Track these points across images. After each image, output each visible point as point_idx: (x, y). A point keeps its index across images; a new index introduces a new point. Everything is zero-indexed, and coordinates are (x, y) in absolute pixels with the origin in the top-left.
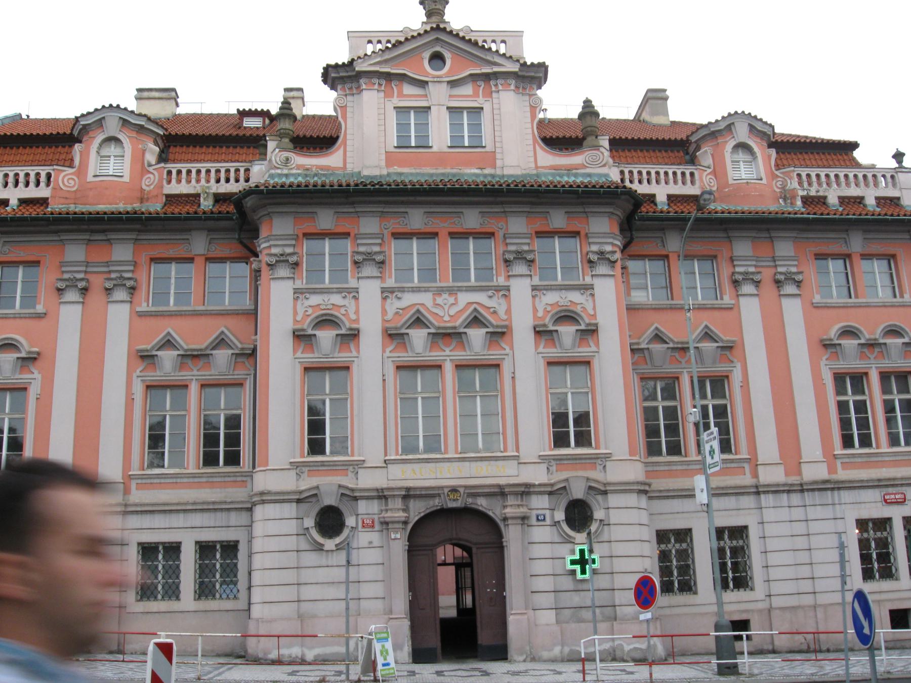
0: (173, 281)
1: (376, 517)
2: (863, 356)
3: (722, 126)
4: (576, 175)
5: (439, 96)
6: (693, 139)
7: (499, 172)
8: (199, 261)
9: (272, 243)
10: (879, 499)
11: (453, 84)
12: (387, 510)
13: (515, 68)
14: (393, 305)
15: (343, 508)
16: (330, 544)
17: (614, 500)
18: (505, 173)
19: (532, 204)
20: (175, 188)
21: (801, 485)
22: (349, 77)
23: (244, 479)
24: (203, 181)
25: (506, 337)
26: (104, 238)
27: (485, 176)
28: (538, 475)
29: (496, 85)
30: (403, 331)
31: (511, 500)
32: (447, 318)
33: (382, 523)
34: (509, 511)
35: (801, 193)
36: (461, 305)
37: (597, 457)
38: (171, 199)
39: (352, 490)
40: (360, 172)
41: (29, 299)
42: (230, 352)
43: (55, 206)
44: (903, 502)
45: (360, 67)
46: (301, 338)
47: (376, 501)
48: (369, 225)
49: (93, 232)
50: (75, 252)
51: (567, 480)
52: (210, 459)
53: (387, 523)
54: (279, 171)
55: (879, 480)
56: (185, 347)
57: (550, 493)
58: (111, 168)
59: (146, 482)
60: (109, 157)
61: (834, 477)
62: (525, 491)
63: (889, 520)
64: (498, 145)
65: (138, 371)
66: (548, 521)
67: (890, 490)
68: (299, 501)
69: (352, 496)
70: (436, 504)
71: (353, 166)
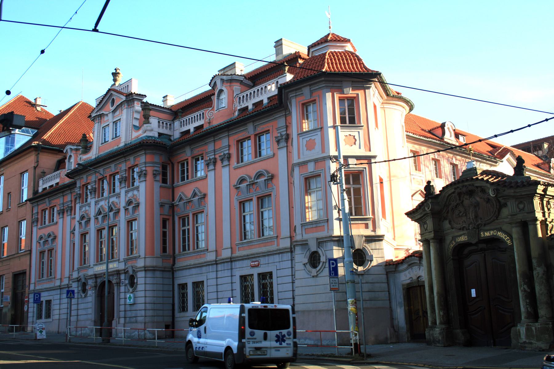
11: (114, 111)
35: (239, 108)
49: (63, 192)
55: (248, 255)
61: (234, 255)
63: (253, 275)
67: (254, 260)
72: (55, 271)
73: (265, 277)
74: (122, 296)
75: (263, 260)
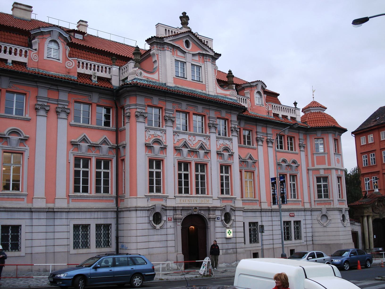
0: (82, 112)
1: (172, 217)
2: (286, 169)
3: (255, 84)
4: (228, 98)
5: (189, 58)
6: (243, 86)
7: (207, 93)
8: (94, 105)
9: (137, 107)
10: (288, 215)
11: (194, 55)
12: (176, 215)
13: (213, 54)
14: (177, 138)
15: (162, 213)
16: (158, 226)
17: (237, 213)
18: (210, 94)
19: (218, 107)
20: (81, 70)
21: (272, 209)
22: (160, 43)
23: (112, 199)
24: (93, 70)
25: (209, 154)
26: (56, 88)
27: (203, 93)
28: (217, 204)
29: (206, 59)
30: (181, 148)
31: (211, 212)
32: (192, 145)
33: (174, 219)
34: (211, 216)
36: (197, 141)
37: (231, 199)
38: (80, 75)
39: (166, 207)
40: (165, 84)
41: (20, 111)
42: (108, 146)
43: (31, 68)
44: (293, 216)
45: (166, 41)
46: (148, 147)
47: (172, 211)
48: (169, 106)
50: (43, 93)
51: (226, 206)
52: (98, 190)
53: (176, 219)
54: (139, 77)
56: (92, 143)
57: (221, 210)
58: (52, 54)
59: (75, 199)
60: (51, 48)
62: (215, 209)
64: (207, 82)
65: (71, 150)
66: (220, 220)
68: (148, 210)
69: (165, 209)
70: (189, 212)
71: (162, 80)
72: (31, 186)
73: (298, 223)
74: (218, 230)
75: (296, 213)
